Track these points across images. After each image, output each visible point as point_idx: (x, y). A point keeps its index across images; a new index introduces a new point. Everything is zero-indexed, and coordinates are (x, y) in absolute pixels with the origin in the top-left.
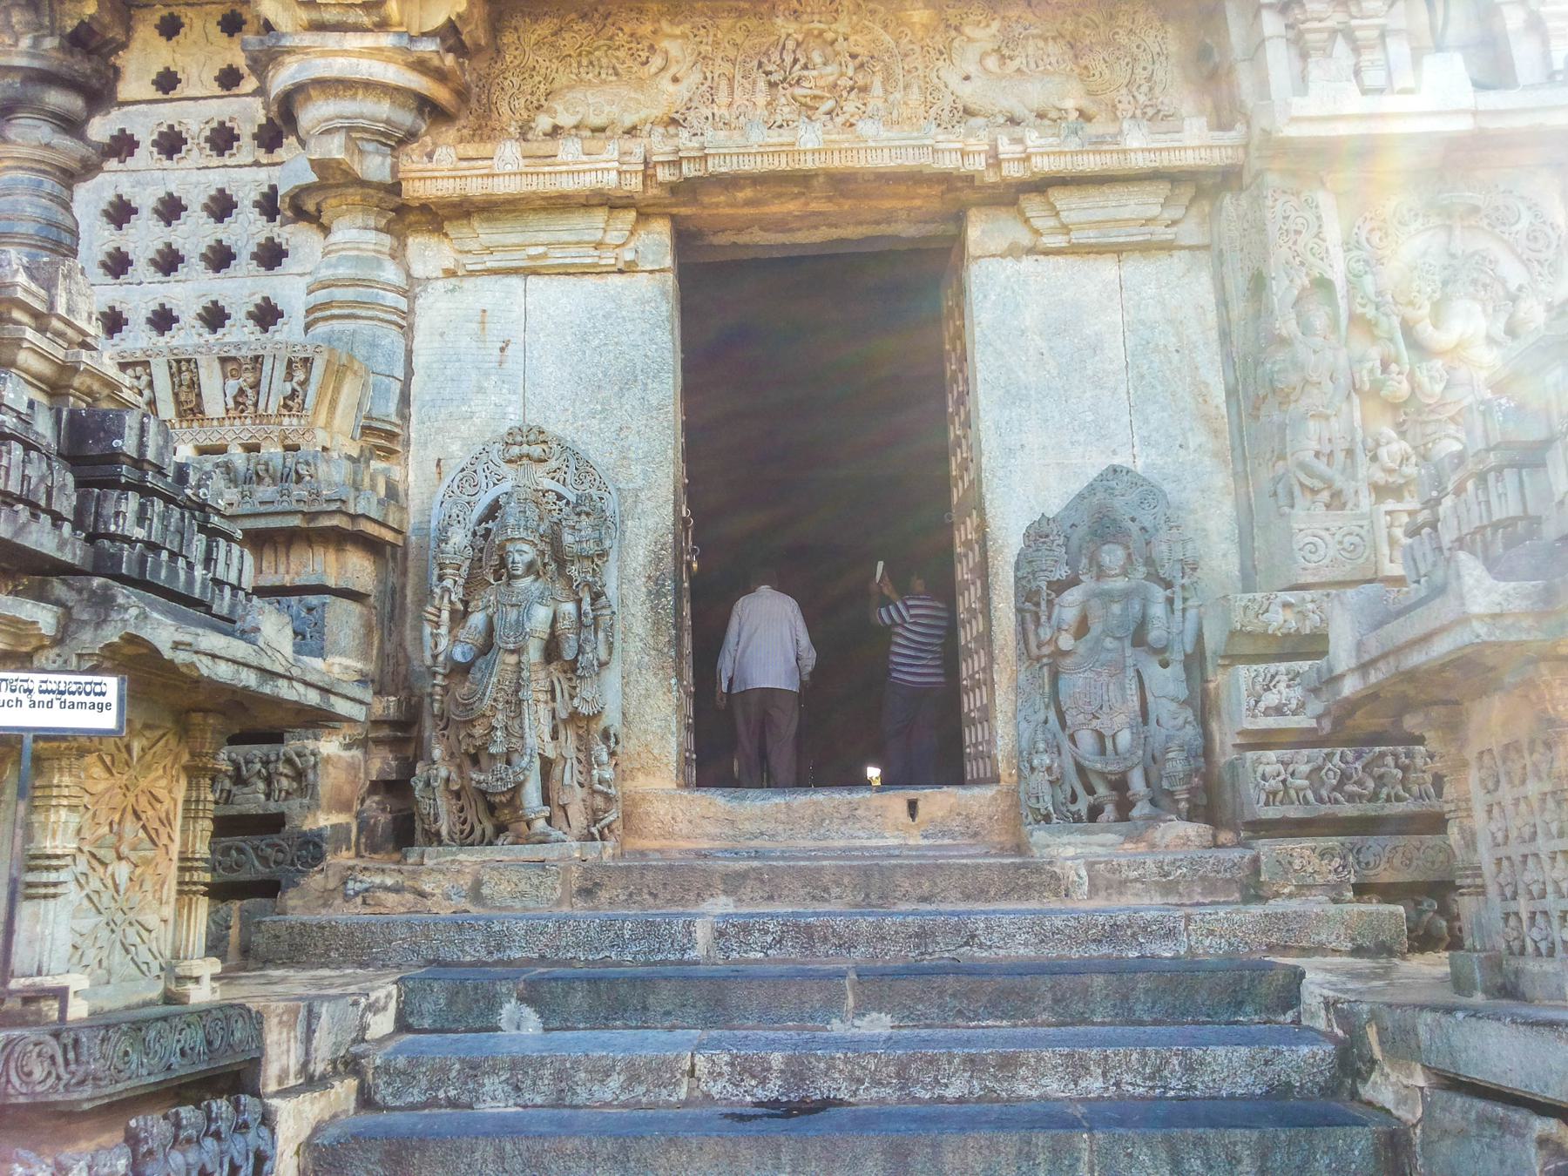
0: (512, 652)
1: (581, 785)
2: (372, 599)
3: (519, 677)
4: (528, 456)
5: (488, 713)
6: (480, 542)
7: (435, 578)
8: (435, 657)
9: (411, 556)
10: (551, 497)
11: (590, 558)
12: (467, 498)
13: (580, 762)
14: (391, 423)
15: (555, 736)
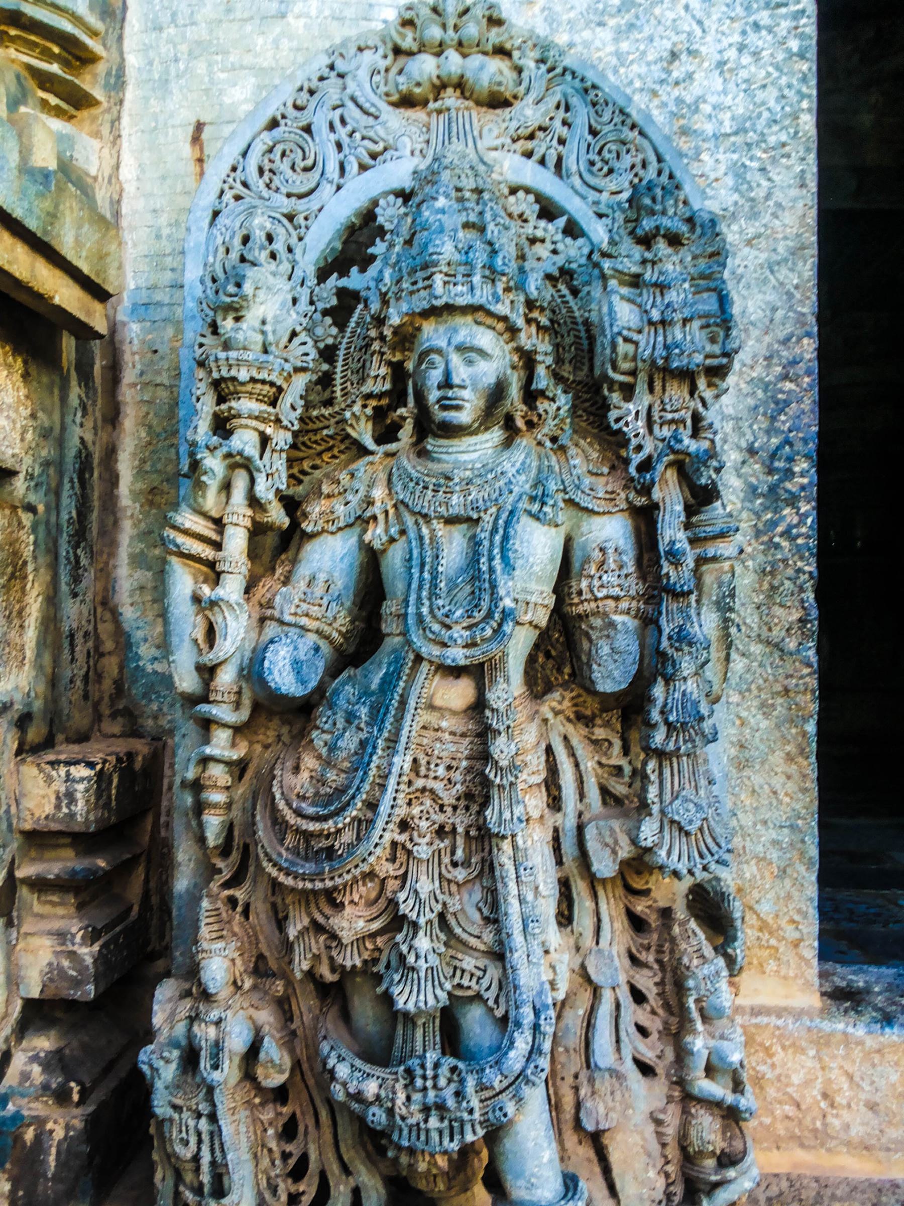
0: (456, 672)
1: (646, 1069)
2: (20, 485)
3: (483, 756)
4: (460, 85)
5: (386, 869)
6: (327, 331)
7: (202, 429)
8: (208, 672)
9: (129, 376)
10: (525, 204)
11: (687, 376)
12: (287, 205)
13: (638, 997)
14: (76, 19)
15: (565, 918)
